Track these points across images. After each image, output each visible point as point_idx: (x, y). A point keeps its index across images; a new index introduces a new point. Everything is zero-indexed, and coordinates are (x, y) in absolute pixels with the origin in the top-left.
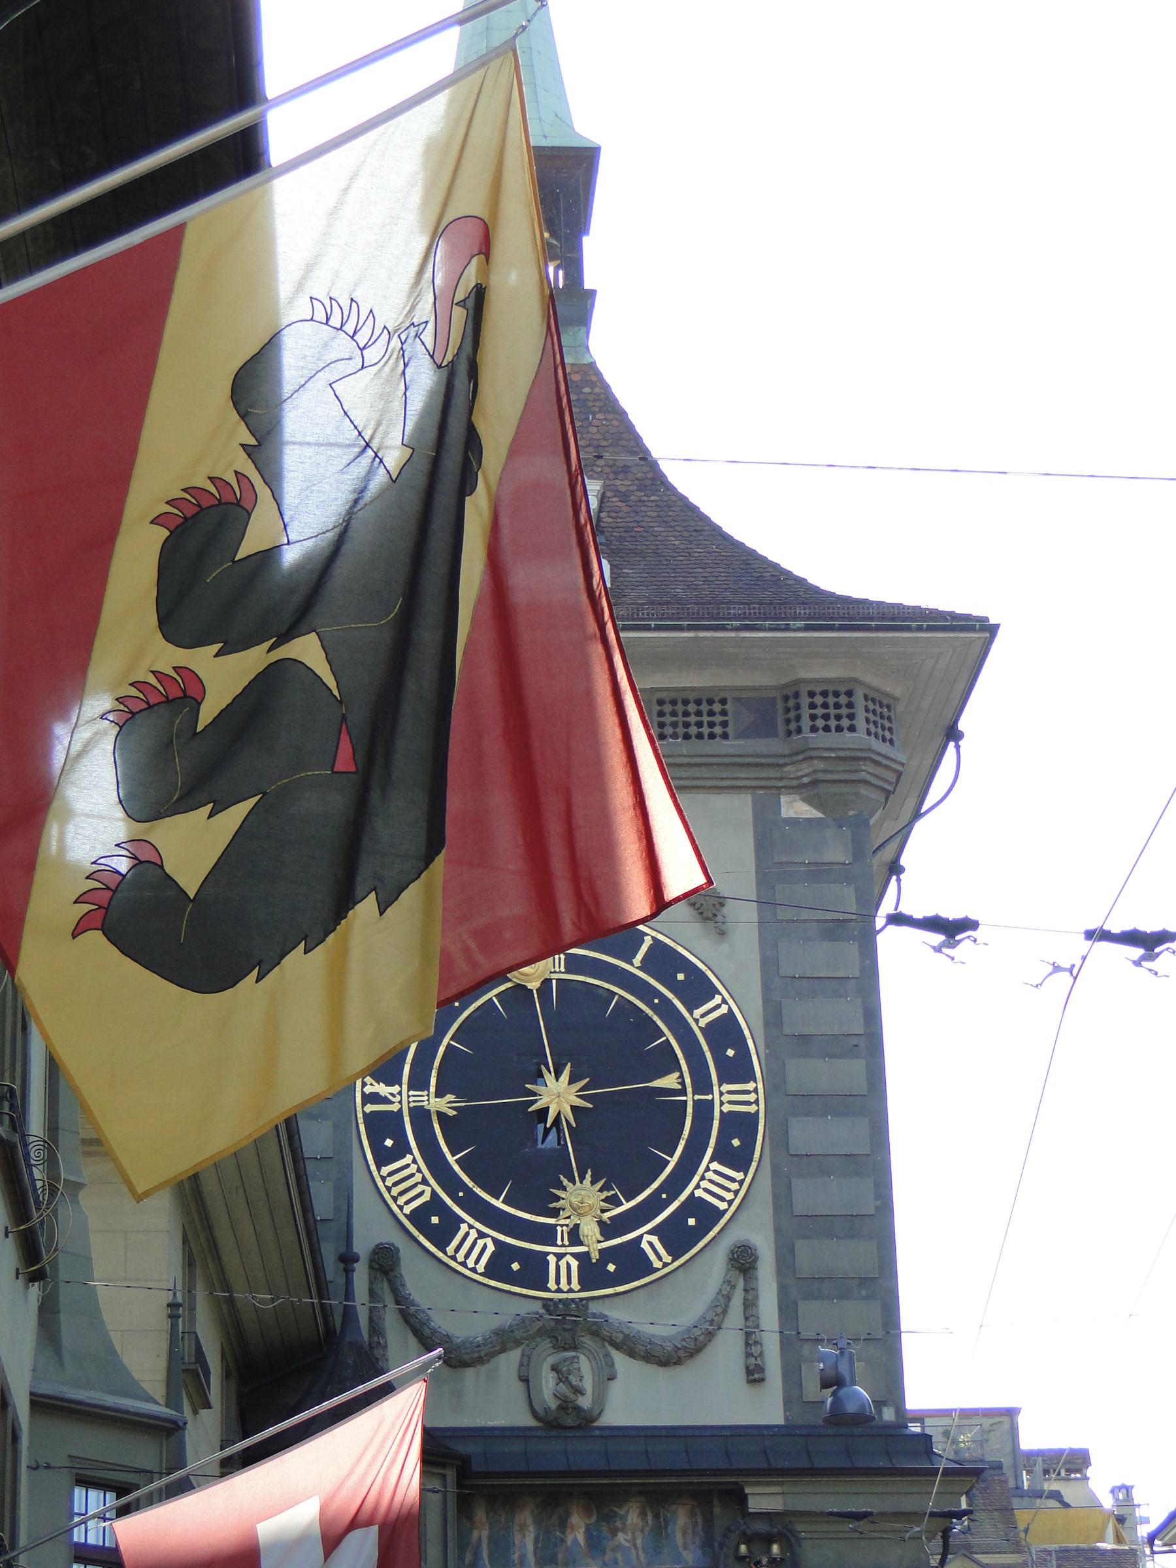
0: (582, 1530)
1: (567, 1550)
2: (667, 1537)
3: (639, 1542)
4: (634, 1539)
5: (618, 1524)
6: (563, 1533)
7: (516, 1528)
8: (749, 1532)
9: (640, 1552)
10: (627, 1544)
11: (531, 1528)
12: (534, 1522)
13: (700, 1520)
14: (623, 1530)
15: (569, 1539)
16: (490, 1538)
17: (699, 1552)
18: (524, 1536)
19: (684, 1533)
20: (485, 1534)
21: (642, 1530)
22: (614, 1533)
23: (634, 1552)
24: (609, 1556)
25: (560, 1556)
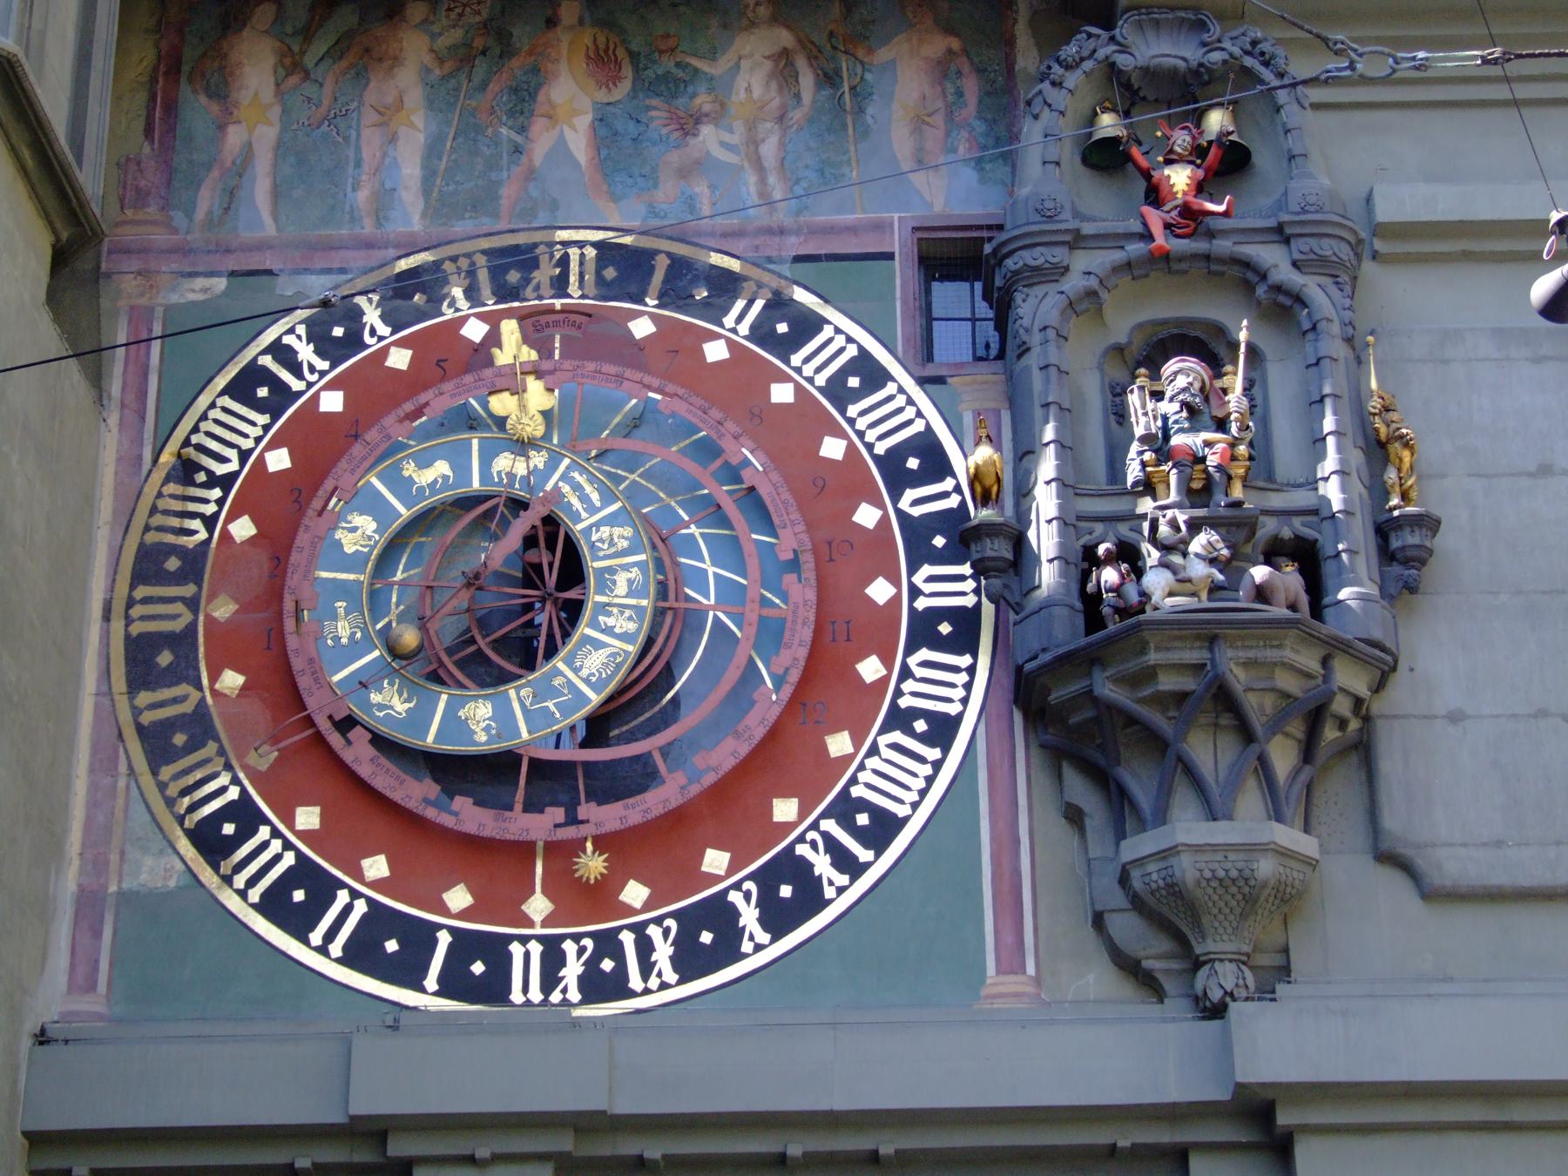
0: (584, 121)
1: (531, 175)
2: (864, 133)
3: (769, 149)
4: (754, 142)
5: (703, 101)
6: (522, 130)
7: (370, 117)
8: (1122, 60)
9: (772, 180)
10: (731, 158)
11: (418, 119)
12: (430, 104)
13: (971, 87)
14: (719, 115)
15: (541, 143)
16: (279, 145)
17: (969, 175)
18: (393, 139)
19: (919, 123)
20: (266, 136)
21: (781, 119)
22: (688, 125)
23: (752, 179)
24: (667, 192)
25: (507, 193)
